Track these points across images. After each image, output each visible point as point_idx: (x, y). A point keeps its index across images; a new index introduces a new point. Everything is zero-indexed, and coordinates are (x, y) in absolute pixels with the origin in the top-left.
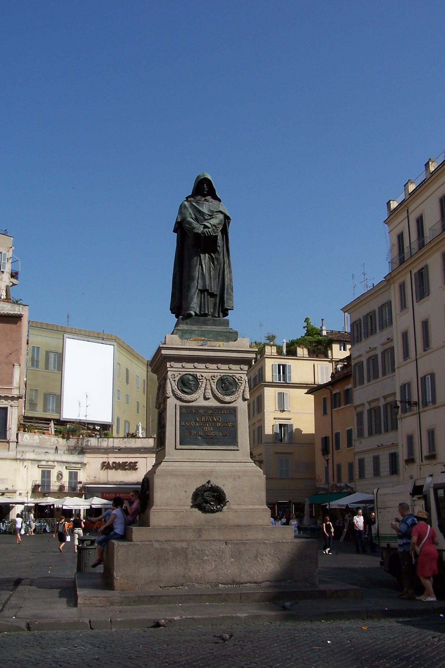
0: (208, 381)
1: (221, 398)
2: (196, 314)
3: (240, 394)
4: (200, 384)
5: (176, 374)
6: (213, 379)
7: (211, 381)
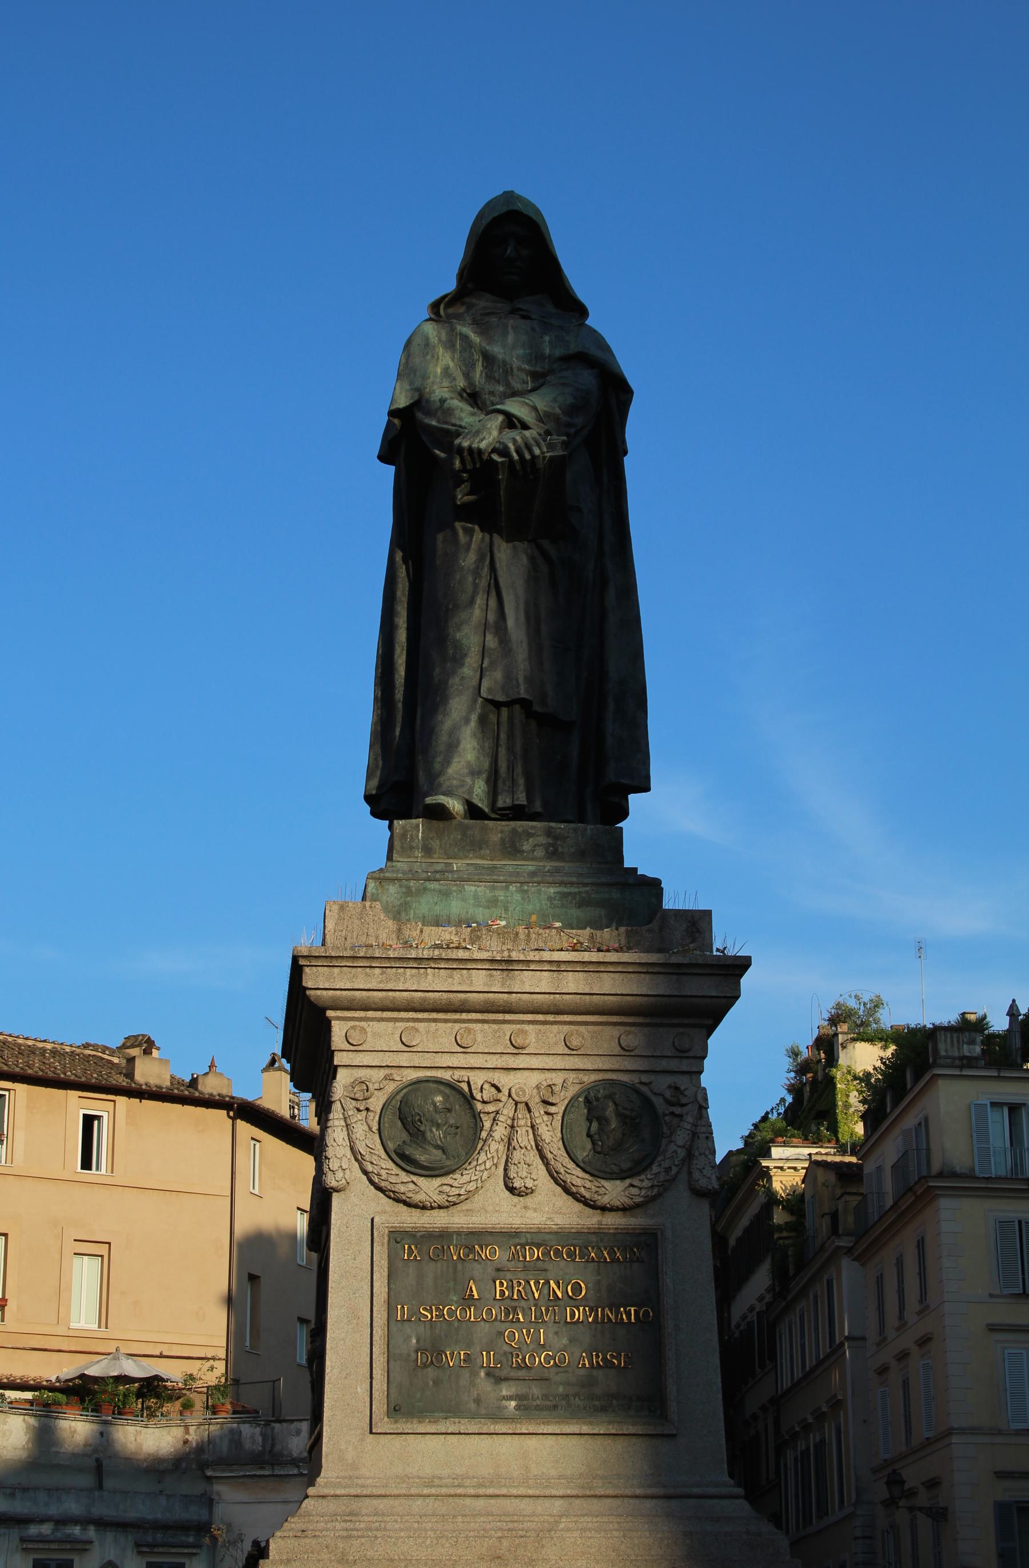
2: (473, 812)
3: (674, 1170)
4: (487, 1125)
6: (546, 1102)
7: (538, 1110)
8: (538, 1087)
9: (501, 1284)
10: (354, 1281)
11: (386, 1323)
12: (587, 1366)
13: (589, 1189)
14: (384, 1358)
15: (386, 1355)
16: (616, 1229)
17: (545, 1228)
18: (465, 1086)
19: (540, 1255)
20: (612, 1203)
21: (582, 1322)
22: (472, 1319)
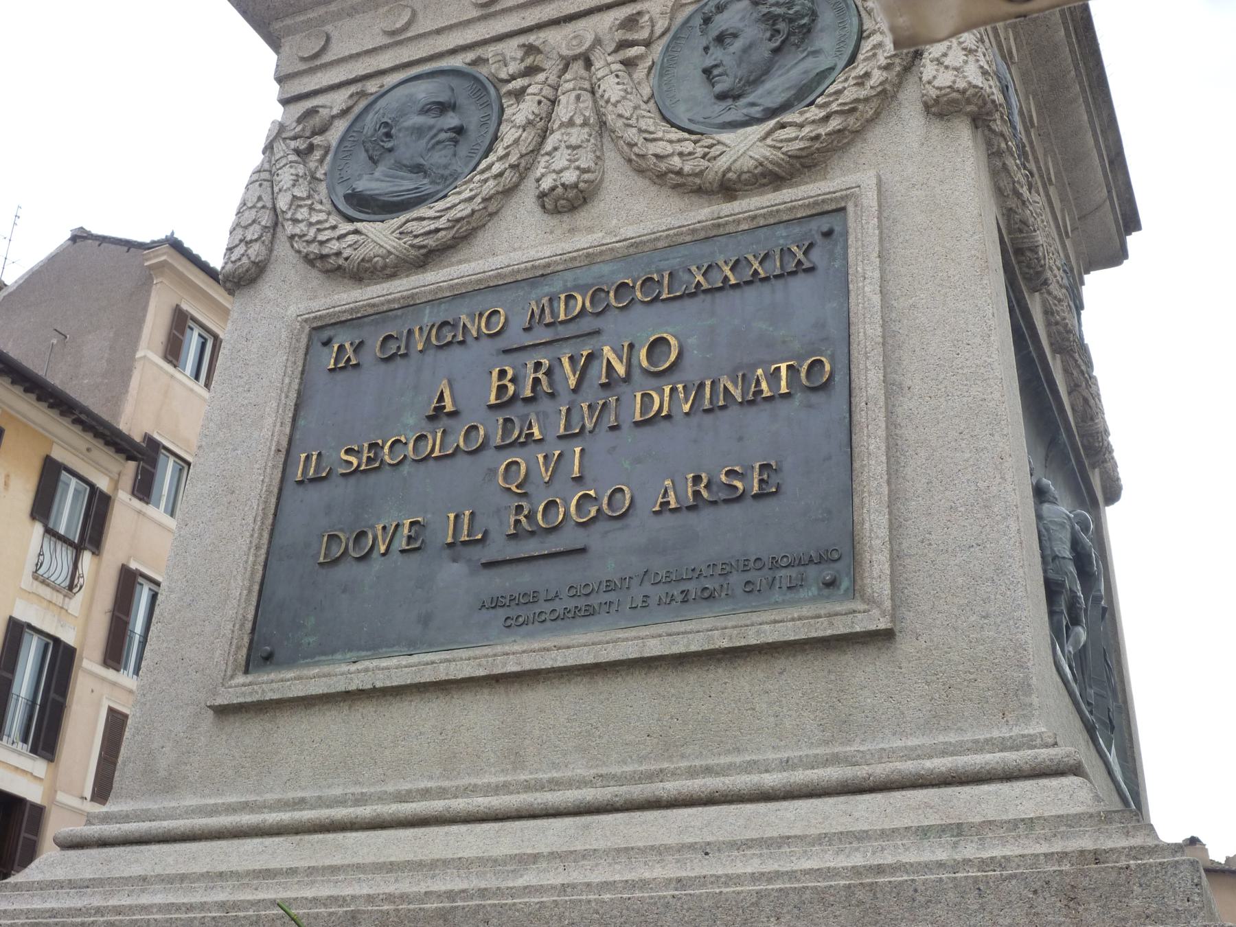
0: (577, 68)
1: (676, 162)
5: (338, 100)
8: (611, 28)
9: (502, 373)
10: (239, 428)
11: (276, 491)
12: (673, 505)
13: (690, 154)
14: (256, 556)
15: (263, 551)
16: (754, 218)
17: (601, 253)
18: (483, 71)
19: (588, 304)
20: (737, 165)
21: (668, 417)
22: (436, 453)
